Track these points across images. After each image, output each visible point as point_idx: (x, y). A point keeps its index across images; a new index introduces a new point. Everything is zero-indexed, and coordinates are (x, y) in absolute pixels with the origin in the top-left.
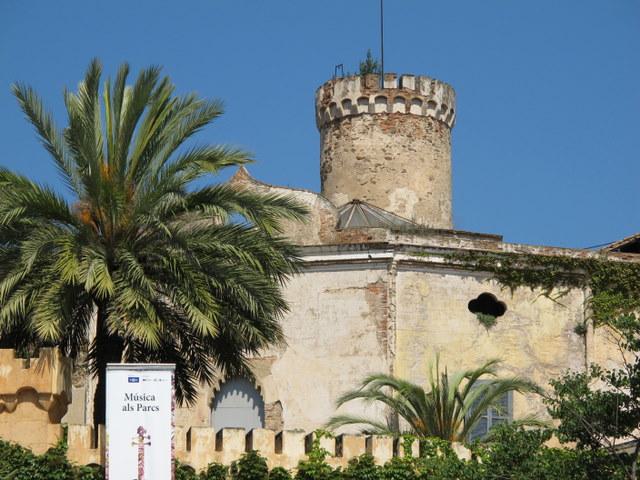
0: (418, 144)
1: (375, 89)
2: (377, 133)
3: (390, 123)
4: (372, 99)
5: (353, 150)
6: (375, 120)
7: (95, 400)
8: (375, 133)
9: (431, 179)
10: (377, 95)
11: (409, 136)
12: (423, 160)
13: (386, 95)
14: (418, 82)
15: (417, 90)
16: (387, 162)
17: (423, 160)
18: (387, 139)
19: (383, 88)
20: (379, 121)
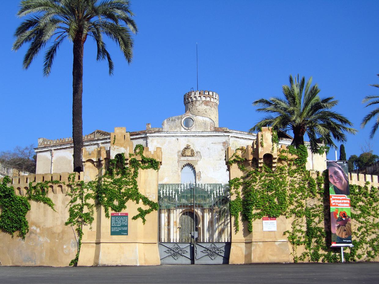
0: (213, 109)
1: (203, 94)
2: (203, 105)
3: (206, 103)
4: (202, 96)
5: (197, 109)
6: (202, 102)
7: (74, 163)
8: (203, 105)
9: (215, 118)
10: (203, 96)
11: (211, 107)
12: (214, 113)
13: (206, 96)
14: (213, 93)
15: (213, 95)
16: (206, 113)
17: (214, 113)
18: (206, 107)
19: (205, 94)
20: (204, 103)
